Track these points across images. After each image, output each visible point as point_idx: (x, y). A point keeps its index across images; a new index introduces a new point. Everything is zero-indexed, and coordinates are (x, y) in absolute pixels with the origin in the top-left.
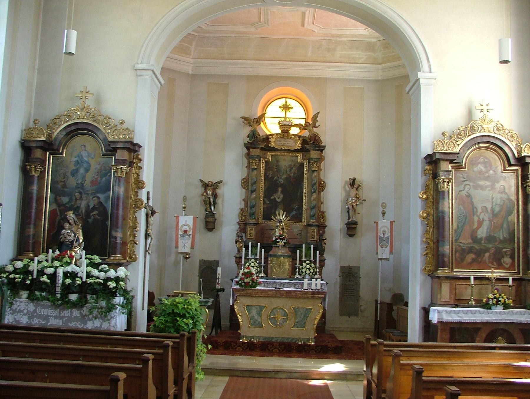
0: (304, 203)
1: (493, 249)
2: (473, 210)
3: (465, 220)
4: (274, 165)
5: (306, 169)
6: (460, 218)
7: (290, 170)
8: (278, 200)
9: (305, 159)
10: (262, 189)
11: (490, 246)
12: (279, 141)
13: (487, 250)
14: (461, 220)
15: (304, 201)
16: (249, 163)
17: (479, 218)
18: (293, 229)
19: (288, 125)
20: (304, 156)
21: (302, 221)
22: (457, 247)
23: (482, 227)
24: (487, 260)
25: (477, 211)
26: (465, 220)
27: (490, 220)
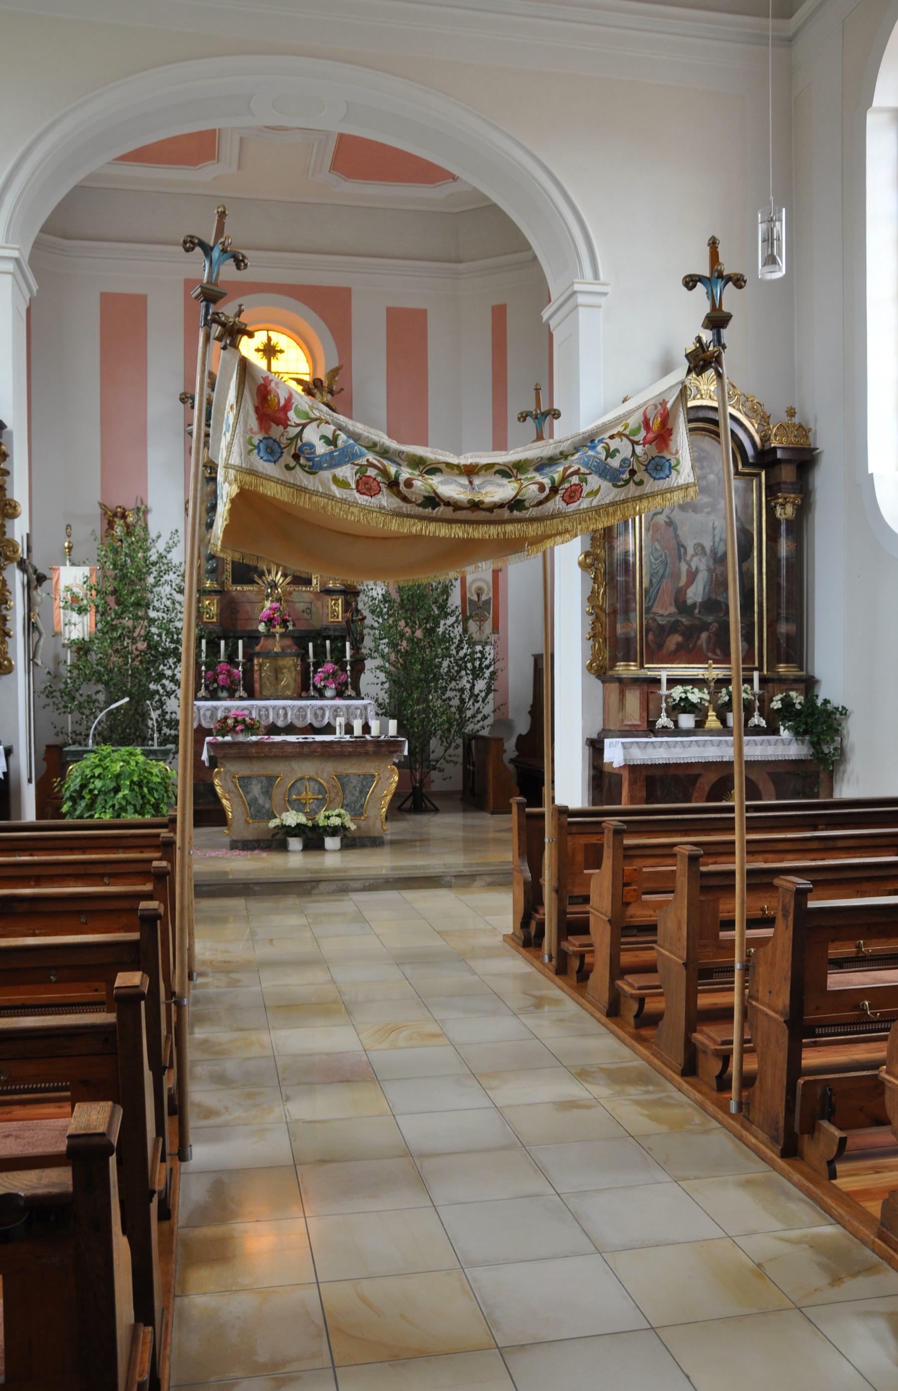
1: (714, 624)
2: (679, 550)
3: (664, 571)
6: (654, 567)
11: (710, 619)
13: (705, 627)
14: (656, 571)
17: (690, 566)
22: (650, 621)
23: (695, 583)
24: (704, 646)
25: (686, 552)
26: (664, 571)
27: (709, 570)
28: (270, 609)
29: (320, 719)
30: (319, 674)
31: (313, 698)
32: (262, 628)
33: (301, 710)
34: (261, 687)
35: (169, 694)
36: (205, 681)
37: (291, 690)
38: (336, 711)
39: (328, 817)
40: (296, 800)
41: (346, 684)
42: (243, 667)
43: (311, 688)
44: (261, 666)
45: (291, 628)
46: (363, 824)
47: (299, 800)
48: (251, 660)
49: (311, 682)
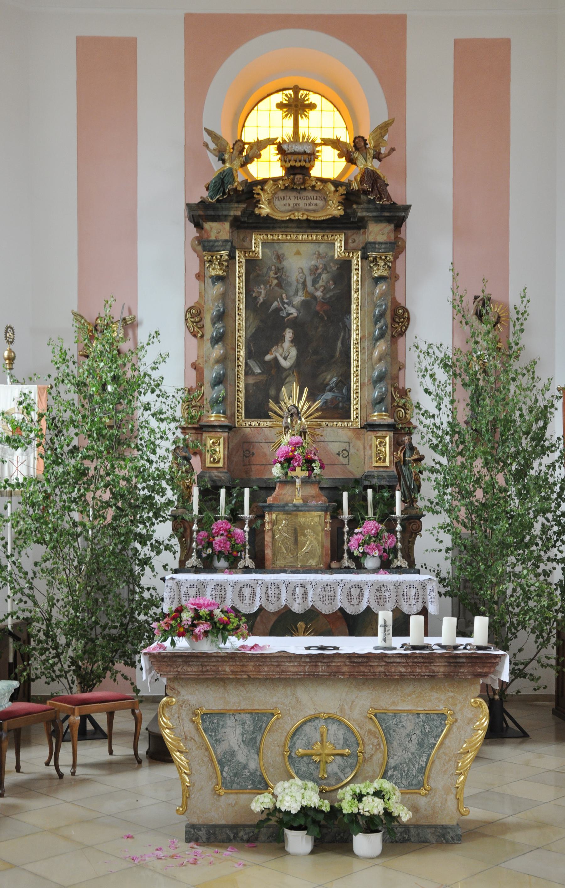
0: (353, 370)
4: (271, 270)
5: (355, 277)
7: (315, 282)
8: (285, 364)
9: (355, 250)
10: (242, 334)
12: (283, 199)
15: (354, 364)
16: (202, 262)
18: (327, 440)
19: (305, 153)
20: (350, 241)
21: (349, 417)
28: (289, 443)
29: (355, 601)
30: (355, 536)
31: (347, 570)
32: (276, 471)
33: (328, 588)
34: (274, 555)
35: (146, 562)
36: (197, 545)
37: (317, 559)
38: (379, 590)
39: (360, 797)
40: (302, 756)
41: (394, 550)
42: (249, 526)
43: (346, 556)
44: (273, 523)
45: (317, 471)
46: (422, 802)
47: (309, 756)
48: (263, 517)
49: (345, 547)
